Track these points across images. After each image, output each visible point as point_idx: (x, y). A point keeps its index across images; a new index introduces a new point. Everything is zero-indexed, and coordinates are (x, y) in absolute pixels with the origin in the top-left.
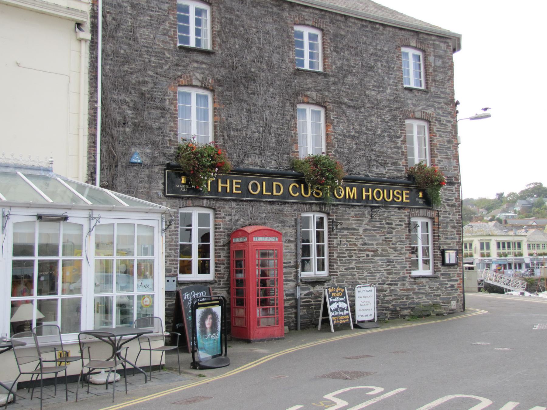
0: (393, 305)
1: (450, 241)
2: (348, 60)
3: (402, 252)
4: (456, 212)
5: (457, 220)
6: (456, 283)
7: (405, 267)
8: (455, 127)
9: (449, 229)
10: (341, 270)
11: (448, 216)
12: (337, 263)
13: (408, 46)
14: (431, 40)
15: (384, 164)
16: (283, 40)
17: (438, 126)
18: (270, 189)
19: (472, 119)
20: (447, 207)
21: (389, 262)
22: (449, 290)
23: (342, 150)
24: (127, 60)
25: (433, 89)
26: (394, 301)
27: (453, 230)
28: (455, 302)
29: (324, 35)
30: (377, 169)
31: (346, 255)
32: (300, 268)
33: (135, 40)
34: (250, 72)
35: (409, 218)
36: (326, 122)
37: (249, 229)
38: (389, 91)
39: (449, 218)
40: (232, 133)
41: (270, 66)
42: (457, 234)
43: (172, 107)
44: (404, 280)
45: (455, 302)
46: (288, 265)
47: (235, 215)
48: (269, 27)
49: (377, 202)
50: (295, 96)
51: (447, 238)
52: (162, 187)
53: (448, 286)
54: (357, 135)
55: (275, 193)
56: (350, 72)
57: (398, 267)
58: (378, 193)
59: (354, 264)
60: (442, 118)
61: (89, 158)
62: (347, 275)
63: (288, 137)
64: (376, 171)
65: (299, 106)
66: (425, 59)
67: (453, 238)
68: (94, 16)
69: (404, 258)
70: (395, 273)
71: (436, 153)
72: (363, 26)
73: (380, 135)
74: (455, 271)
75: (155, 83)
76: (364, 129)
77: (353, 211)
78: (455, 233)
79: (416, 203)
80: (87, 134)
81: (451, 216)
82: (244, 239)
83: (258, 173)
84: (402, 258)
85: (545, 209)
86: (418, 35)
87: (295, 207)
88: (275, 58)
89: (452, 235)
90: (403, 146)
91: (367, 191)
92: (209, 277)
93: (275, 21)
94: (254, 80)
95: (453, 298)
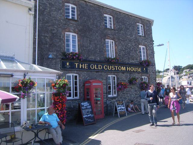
8: (153, 48)
13: (139, 23)
15: (133, 60)
16: (100, 19)
17: (149, 48)
18: (97, 67)
19: (158, 46)
21: (136, 91)
24: (47, 22)
25: (146, 36)
29: (113, 18)
32: (108, 94)
33: (50, 15)
34: (90, 28)
35: (141, 77)
36: (115, 45)
37: (91, 81)
38: (134, 36)
40: (84, 48)
41: (97, 26)
43: (63, 39)
47: (86, 76)
48: (96, 14)
49: (132, 72)
50: (105, 36)
52: (60, 66)
55: (99, 69)
56: (121, 30)
58: (132, 69)
61: (33, 56)
63: (103, 49)
64: (131, 61)
65: (106, 40)
66: (144, 27)
68: (35, 6)
72: (126, 16)
75: (57, 30)
76: (127, 48)
79: (143, 72)
80: (32, 47)
82: (89, 84)
83: (93, 61)
87: (106, 73)
88: (99, 24)
91: (129, 68)
92: (78, 97)
94: (91, 31)
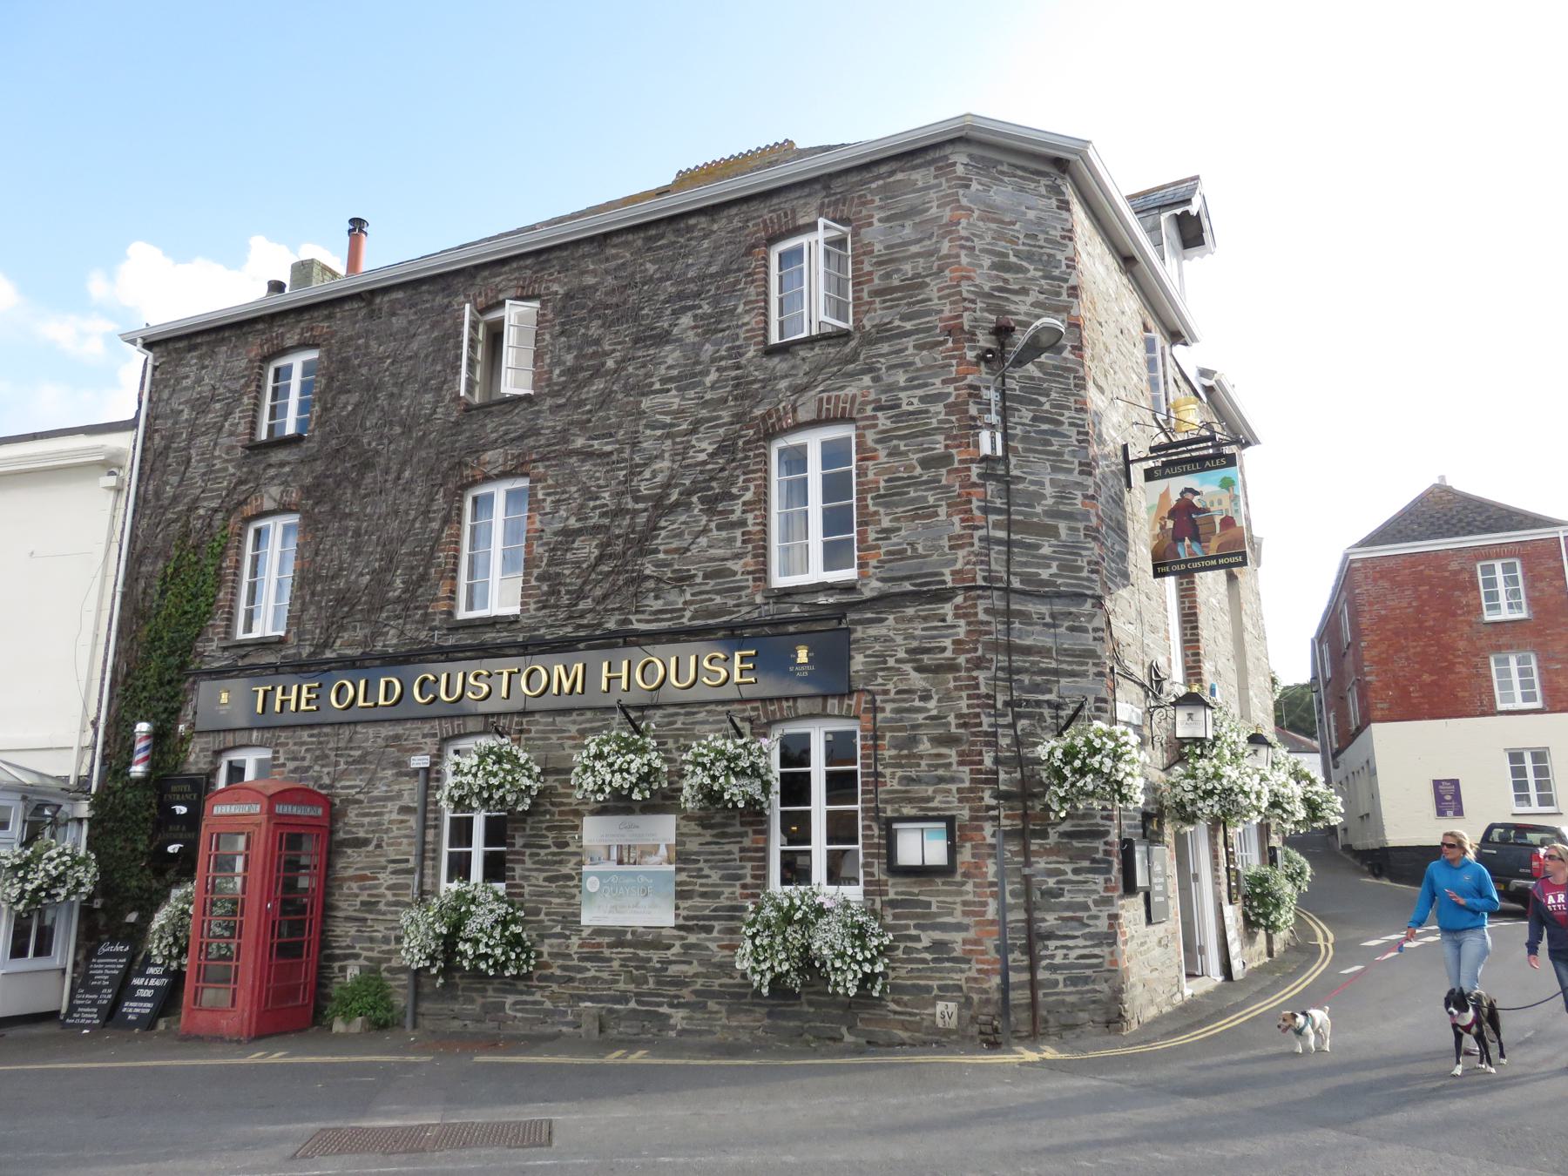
0: (696, 992)
1: (930, 790)
2: (597, 342)
3: (730, 830)
4: (957, 688)
5: (959, 716)
6: (958, 937)
7: (739, 877)
9: (925, 747)
10: (534, 881)
11: (917, 703)
12: (523, 862)
14: (878, 177)
20: (914, 675)
22: (924, 961)
23: (558, 569)
26: (700, 981)
27: (943, 750)
28: (952, 1006)
30: (657, 598)
31: (549, 842)
39: (926, 710)
42: (961, 763)
44: (732, 918)
45: (952, 1006)
46: (403, 866)
51: (918, 781)
53: (919, 946)
54: (607, 521)
56: (597, 372)
57: (715, 876)
59: (571, 865)
60: (902, 395)
62: (550, 894)
67: (941, 780)
69: (735, 848)
70: (704, 895)
71: (872, 509)
73: (677, 504)
74: (948, 893)
77: (574, 722)
78: (954, 759)
81: (932, 704)
84: (727, 848)
85: (1413, 624)
86: (827, 187)
89: (937, 767)
90: (750, 516)
93: (433, 327)
95: (940, 988)
